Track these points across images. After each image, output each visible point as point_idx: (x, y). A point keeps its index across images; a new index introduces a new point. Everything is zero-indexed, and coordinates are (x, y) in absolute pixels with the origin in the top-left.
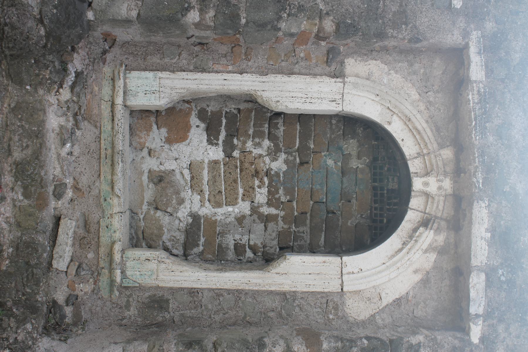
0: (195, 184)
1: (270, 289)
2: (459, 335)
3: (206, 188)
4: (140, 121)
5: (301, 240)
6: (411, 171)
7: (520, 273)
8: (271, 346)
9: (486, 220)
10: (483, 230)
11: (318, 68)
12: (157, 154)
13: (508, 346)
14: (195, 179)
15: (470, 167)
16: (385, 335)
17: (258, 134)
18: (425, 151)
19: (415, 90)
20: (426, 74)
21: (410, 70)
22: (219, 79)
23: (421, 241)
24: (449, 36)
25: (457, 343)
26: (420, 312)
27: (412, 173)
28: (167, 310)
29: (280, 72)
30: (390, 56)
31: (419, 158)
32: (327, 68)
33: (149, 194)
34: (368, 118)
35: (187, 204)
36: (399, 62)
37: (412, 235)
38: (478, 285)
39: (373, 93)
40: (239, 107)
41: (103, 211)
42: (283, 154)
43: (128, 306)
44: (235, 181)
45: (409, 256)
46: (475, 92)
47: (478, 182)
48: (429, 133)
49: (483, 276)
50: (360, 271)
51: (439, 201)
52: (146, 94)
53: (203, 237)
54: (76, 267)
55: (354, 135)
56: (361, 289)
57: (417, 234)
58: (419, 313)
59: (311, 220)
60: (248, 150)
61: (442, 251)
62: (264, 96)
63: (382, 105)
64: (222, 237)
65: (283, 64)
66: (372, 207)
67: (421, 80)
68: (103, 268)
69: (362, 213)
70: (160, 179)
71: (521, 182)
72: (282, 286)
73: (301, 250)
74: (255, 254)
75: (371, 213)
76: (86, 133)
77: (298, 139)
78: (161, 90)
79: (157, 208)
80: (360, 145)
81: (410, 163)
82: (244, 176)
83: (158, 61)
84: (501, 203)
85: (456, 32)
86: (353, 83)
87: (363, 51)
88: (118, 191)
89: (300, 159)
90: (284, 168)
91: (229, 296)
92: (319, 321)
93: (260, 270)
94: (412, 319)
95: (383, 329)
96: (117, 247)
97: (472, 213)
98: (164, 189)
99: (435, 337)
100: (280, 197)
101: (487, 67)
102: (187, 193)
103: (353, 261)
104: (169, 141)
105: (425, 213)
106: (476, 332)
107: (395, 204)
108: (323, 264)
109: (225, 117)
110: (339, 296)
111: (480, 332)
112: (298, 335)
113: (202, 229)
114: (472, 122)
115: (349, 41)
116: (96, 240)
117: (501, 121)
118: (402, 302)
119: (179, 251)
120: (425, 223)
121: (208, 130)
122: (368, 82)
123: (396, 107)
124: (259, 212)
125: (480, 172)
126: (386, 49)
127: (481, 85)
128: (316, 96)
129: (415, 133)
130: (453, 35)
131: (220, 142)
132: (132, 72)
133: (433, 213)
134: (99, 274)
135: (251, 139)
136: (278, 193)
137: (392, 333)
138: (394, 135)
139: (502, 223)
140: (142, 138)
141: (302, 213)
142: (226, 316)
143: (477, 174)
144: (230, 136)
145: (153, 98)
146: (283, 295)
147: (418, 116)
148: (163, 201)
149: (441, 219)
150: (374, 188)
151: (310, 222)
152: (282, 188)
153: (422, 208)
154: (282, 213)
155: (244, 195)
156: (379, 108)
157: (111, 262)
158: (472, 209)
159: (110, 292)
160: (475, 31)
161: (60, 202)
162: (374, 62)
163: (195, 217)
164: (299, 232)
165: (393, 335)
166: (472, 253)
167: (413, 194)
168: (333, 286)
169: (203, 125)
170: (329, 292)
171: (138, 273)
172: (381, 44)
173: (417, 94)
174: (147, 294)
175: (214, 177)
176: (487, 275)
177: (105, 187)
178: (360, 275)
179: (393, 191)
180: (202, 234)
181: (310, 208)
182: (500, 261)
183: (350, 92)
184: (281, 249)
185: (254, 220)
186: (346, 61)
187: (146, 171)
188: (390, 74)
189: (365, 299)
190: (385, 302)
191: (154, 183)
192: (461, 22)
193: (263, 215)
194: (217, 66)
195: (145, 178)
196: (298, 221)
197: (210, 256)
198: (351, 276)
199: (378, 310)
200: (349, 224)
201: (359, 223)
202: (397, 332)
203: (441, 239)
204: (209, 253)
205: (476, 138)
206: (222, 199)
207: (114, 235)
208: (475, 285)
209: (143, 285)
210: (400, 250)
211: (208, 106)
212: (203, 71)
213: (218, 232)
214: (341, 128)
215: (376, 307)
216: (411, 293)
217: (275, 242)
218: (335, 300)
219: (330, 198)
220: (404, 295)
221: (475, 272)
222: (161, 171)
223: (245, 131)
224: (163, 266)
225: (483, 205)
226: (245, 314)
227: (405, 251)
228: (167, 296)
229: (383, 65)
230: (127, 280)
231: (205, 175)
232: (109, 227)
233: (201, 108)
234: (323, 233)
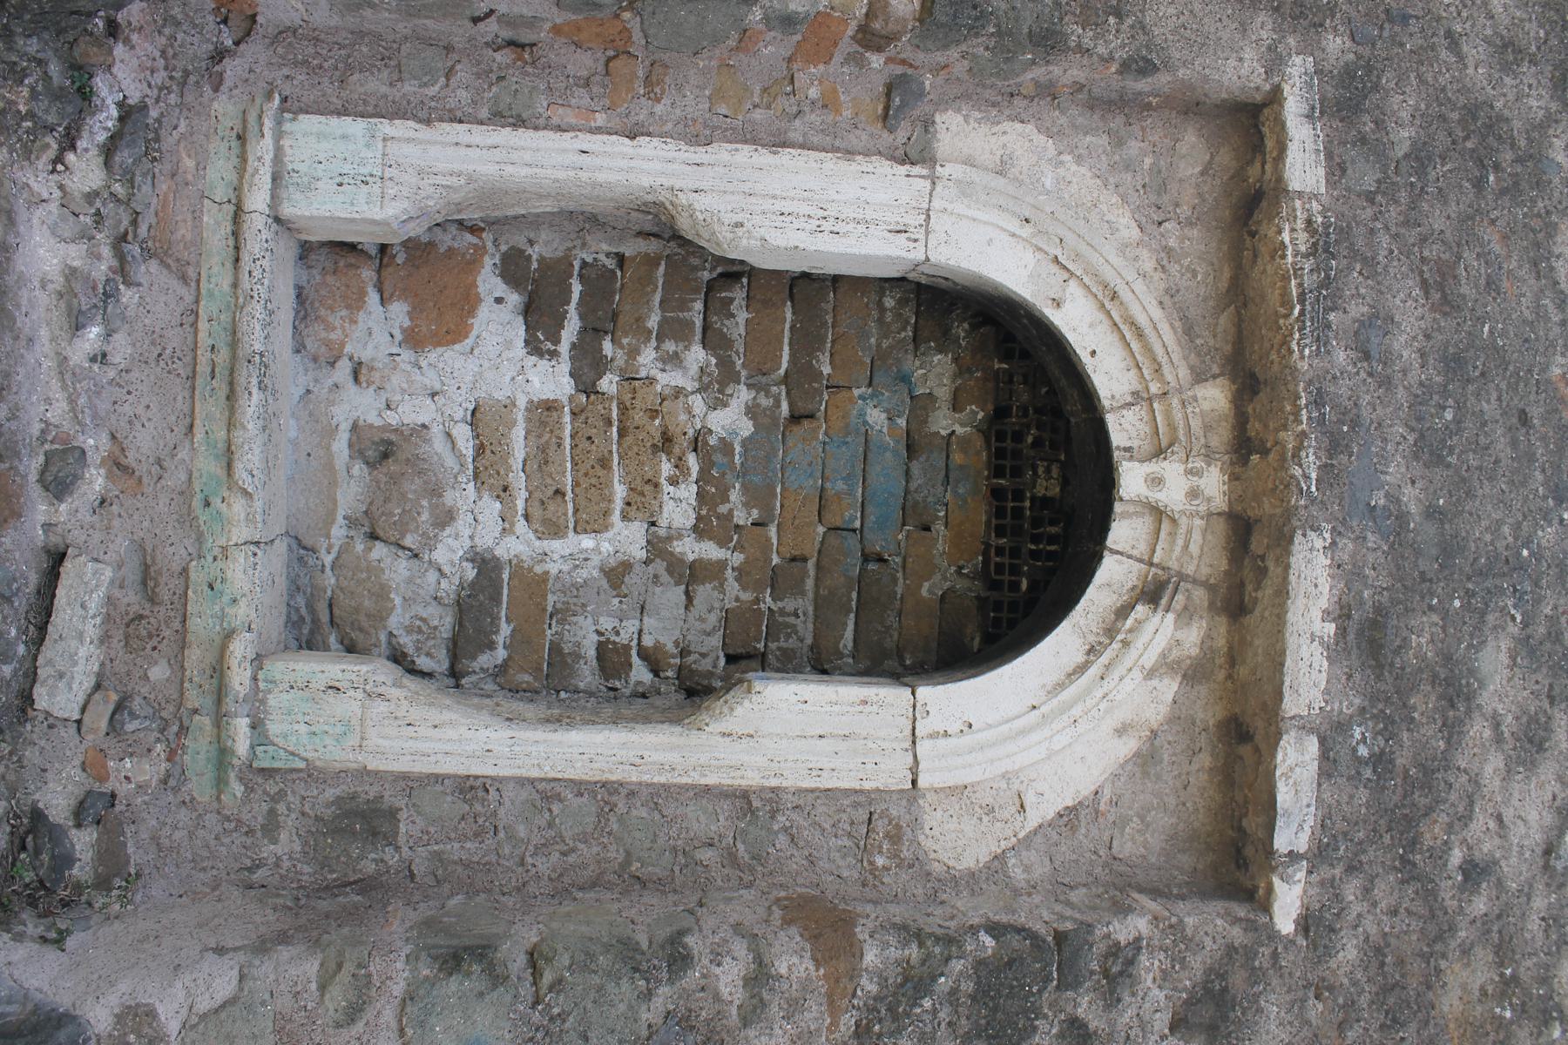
0: (487, 465)
1: (703, 781)
2: (1241, 911)
3: (518, 481)
4: (330, 279)
5: (788, 636)
6: (1114, 444)
7: (1405, 735)
8: (706, 962)
10: (1316, 614)
11: (858, 132)
12: (376, 375)
13: (1367, 939)
14: (488, 452)
15: (1282, 434)
16: (1040, 916)
17: (674, 330)
18: (1154, 388)
19: (1128, 214)
22: (565, 151)
23: (1140, 642)
24: (1232, 62)
25: (1237, 934)
26: (1129, 844)
27: (1118, 448)
28: (391, 840)
29: (749, 137)
30: (1063, 113)
31: (1137, 408)
32: (885, 134)
33: (351, 493)
34: (997, 286)
35: (463, 524)
36: (1086, 134)
38: (1298, 770)
39: (1014, 214)
40: (621, 250)
41: (200, 539)
42: (743, 388)
43: (271, 827)
44: (604, 463)
45: (1107, 685)
46: (1300, 224)
47: (1307, 477)
48: (1166, 338)
49: (1313, 746)
50: (966, 729)
51: (1189, 532)
52: (340, 185)
53: (508, 621)
54: (111, 707)
55: (945, 341)
56: (967, 781)
57: (1129, 622)
58: (1126, 847)
59: (817, 579)
60: (643, 374)
61: (1193, 673)
62: (697, 206)
63: (1040, 249)
64: (561, 622)
65: (758, 115)
66: (987, 546)
67: (1144, 186)
68: (196, 711)
69: (961, 563)
70: (383, 450)
71: (1413, 482)
72: (739, 773)
73: (788, 665)
74: (656, 674)
75: (986, 562)
76: (152, 296)
77: (786, 348)
78: (387, 175)
79: (373, 536)
80: (962, 370)
81: (1110, 419)
82: (630, 448)
83: (384, 89)
84: (1365, 538)
85: (1248, 54)
86: (959, 182)
87: (988, 94)
88: (244, 475)
89: (791, 405)
90: (746, 428)
91: (579, 800)
92: (845, 874)
93: (671, 722)
94: (1105, 865)
95: (1029, 894)
96: (240, 648)
97: (1287, 567)
98: (394, 479)
99: (1181, 921)
100: (731, 510)
101: (1329, 156)
102: (463, 495)
104: (414, 340)
105: (1151, 564)
106: (1288, 901)
107: (1052, 539)
108: (861, 708)
109: (581, 276)
110: (904, 802)
111: (1298, 903)
112: (787, 922)
113: (505, 598)
114: (1292, 308)
115: (954, 53)
116: (177, 625)
117: (1366, 309)
118: (1082, 817)
119: (438, 662)
120: (1152, 593)
121: (528, 311)
122: (1000, 182)
123: (1078, 256)
124: (672, 554)
125: (1311, 451)
126: (1048, 92)
127: (1314, 204)
128: (852, 215)
130: (1241, 60)
131: (564, 348)
132: (301, 117)
133: (1173, 565)
134: (183, 730)
135: (654, 343)
136: (725, 499)
137: (1058, 908)
138: (1071, 337)
139: (1366, 594)
140: (334, 329)
141: (793, 559)
142: (571, 859)
143: (1303, 454)
144: (592, 332)
145: (362, 198)
146: (743, 799)
147: (1139, 286)
148: (392, 514)
149: (1195, 581)
150: (997, 493)
151: (817, 586)
152: (737, 486)
153: (1142, 549)
154: (738, 559)
155: (629, 504)
156: (1029, 257)
157: (220, 692)
158: (1288, 553)
159: (218, 785)
160: (1298, 54)
161: (63, 507)
162: (1018, 126)
163: (486, 565)
164: (782, 612)
165: (1062, 918)
168: (890, 774)
169: (514, 299)
170: (878, 790)
171: (303, 728)
172: (1038, 72)
174: (330, 793)
175: (543, 449)
176: (1322, 741)
177: (207, 466)
178: (967, 739)
179: (1045, 502)
180: (503, 613)
181: (817, 546)
182: (1357, 701)
183: (950, 207)
184: (731, 659)
185: (656, 576)
186: (938, 118)
187: (345, 426)
188: (1061, 163)
189: (977, 808)
190: (1034, 819)
191: (368, 463)
193: (682, 561)
194: (561, 111)
195: (341, 445)
196: (778, 582)
197: (527, 678)
198: (942, 742)
199: (1014, 840)
200: (924, 592)
201: (951, 590)
202: (1068, 903)
203: (1192, 638)
204: (522, 670)
205: (1301, 352)
206: (566, 514)
207: (230, 611)
208: (1291, 769)
209: (318, 763)
210: (1081, 669)
211: (531, 242)
212: (519, 122)
213: (550, 609)
214: (908, 323)
215: (1010, 833)
216: (1107, 793)
217: (716, 641)
218: (894, 813)
219: (872, 518)
220: (1086, 798)
221: (1293, 733)
222: (387, 428)
223: (637, 320)
224: (381, 707)
225: (1319, 544)
226: (628, 854)
227: (1094, 671)
228: (392, 798)
229: (1043, 138)
230: (270, 748)
231: (518, 444)
232: (217, 586)
233: (512, 248)
234: (852, 616)
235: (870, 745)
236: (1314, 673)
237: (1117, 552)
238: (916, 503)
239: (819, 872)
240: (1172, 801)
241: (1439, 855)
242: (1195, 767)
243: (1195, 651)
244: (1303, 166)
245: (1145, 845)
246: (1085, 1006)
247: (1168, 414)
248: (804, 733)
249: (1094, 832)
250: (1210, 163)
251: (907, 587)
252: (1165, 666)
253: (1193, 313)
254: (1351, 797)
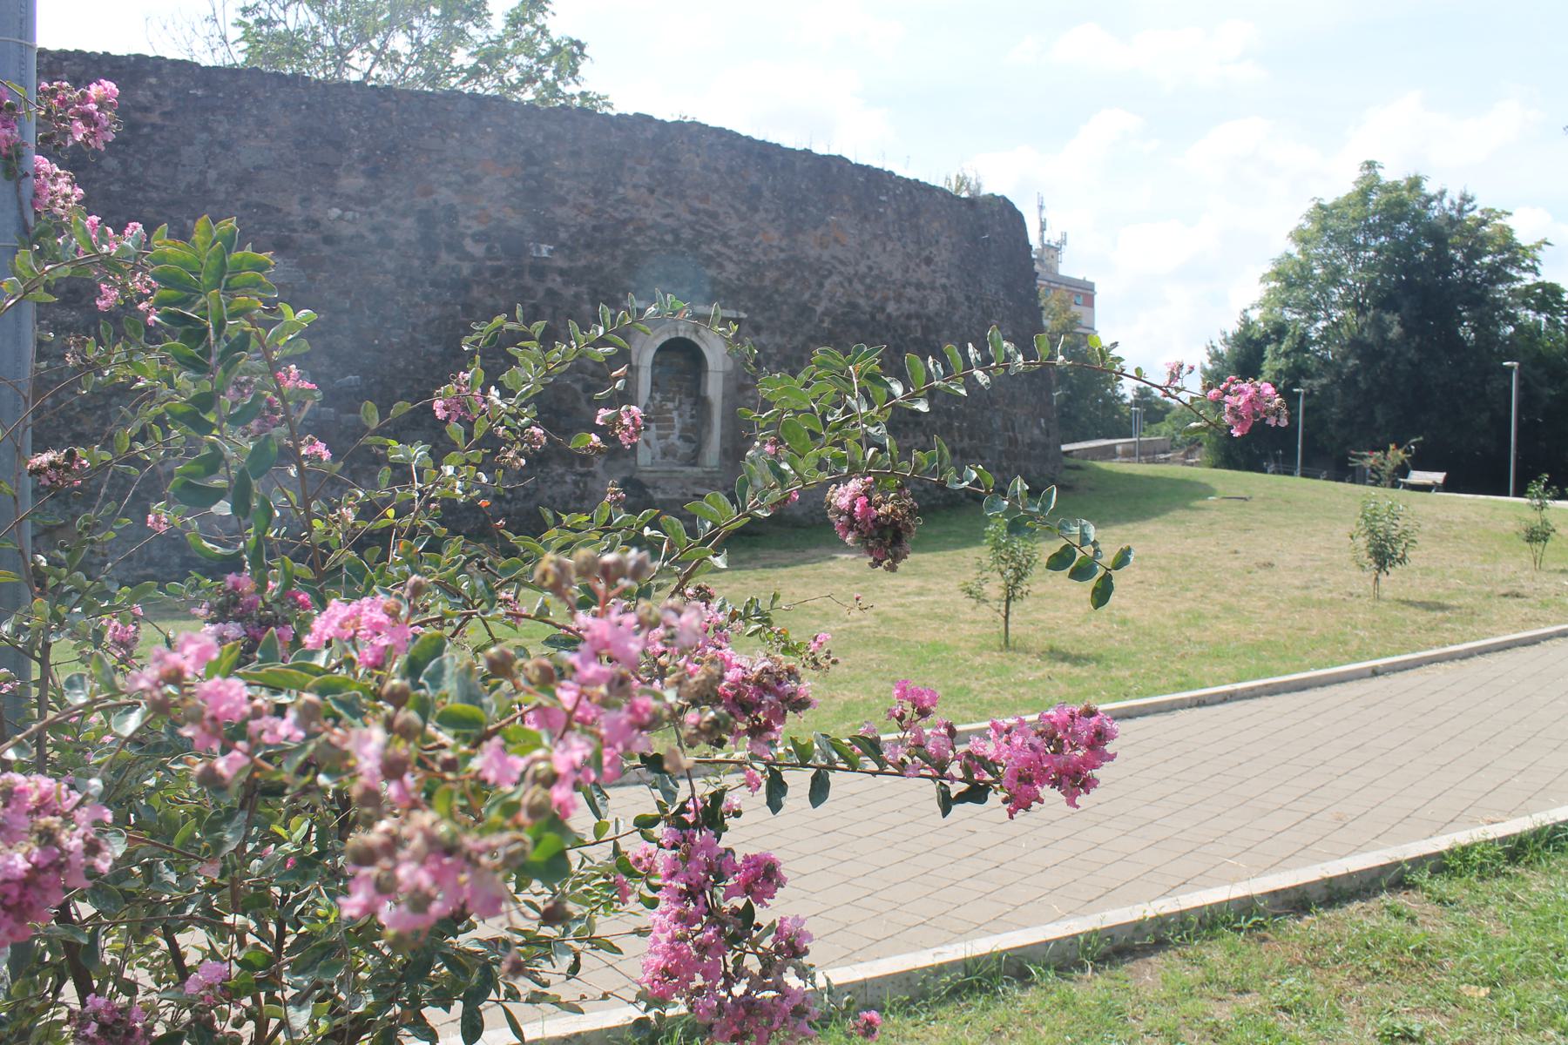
0: (666, 437)
37: (701, 338)
70: (665, 454)
73: (698, 386)
76: (661, 483)
103: (711, 366)
106: (743, 315)
196: (680, 387)
248: (714, 388)
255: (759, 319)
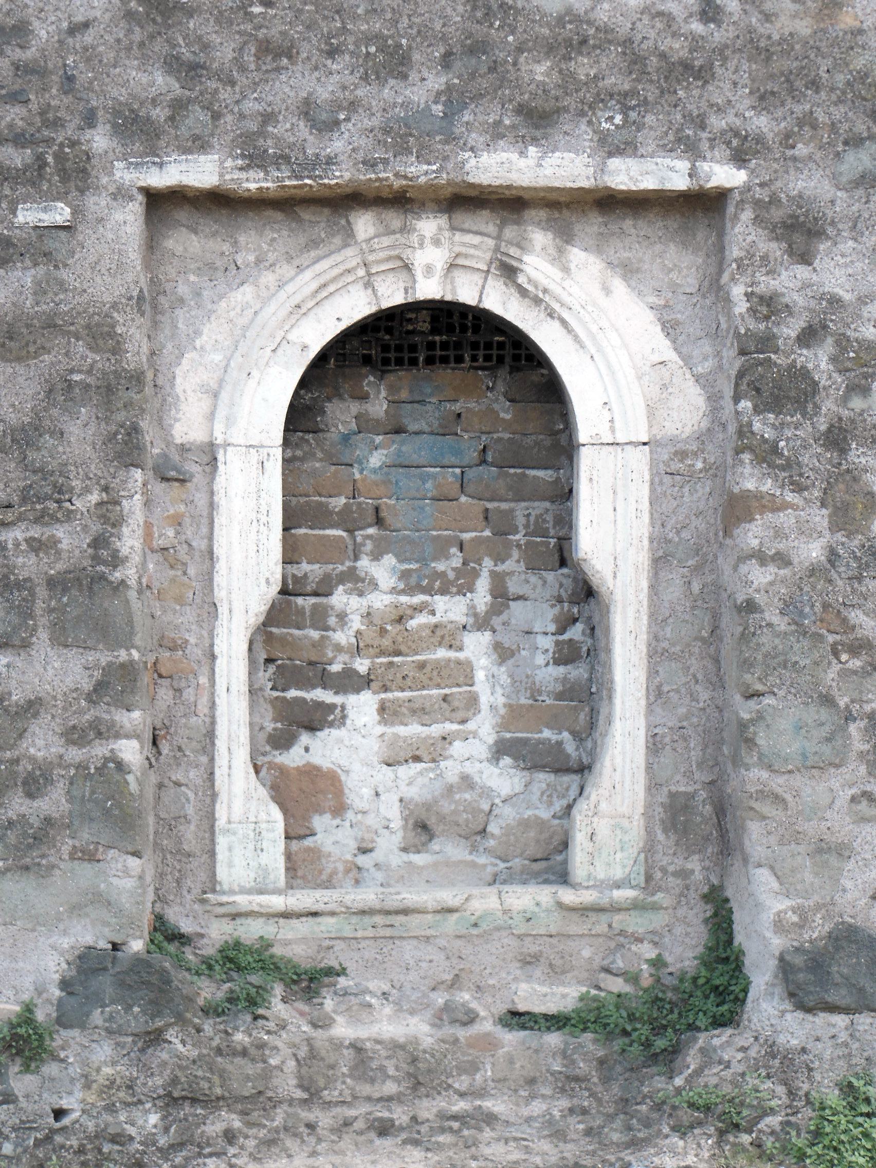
1: (646, 590)
3: (436, 730)
4: (300, 873)
5: (544, 521)
6: (403, 302)
9: (505, 155)
10: (522, 163)
11: (196, 500)
12: (367, 836)
13: (754, 108)
14: (417, 753)
17: (319, 618)
19: (233, 294)
20: (199, 269)
21: (192, 303)
22: (228, 703)
23: (544, 282)
25: (747, 215)
26: (688, 279)
28: (692, 796)
29: (208, 578)
30: (164, 347)
32: (195, 480)
33: (450, 849)
35: (470, 768)
36: (176, 327)
37: (533, 298)
38: (632, 174)
40: (262, 661)
41: (498, 929)
42: (359, 564)
43: (683, 874)
44: (422, 666)
45: (576, 307)
46: (243, 175)
47: (426, 173)
49: (615, 163)
52: (262, 850)
53: (541, 732)
54: (609, 977)
56: (643, 406)
57: (530, 288)
58: (691, 282)
59: (501, 500)
60: (354, 640)
61: (566, 236)
62: (256, 611)
64: (540, 693)
65: (191, 571)
66: (471, 367)
68: (610, 926)
69: (484, 387)
70: (421, 828)
72: (640, 566)
74: (575, 620)
77: (329, 532)
78: (254, 820)
79: (483, 831)
81: (386, 304)
82: (409, 648)
84: (467, 123)
86: (228, 426)
88: (457, 899)
89: (370, 526)
90: (389, 560)
91: (661, 672)
92: (708, 489)
93: (608, 612)
94: (704, 297)
96: (568, 896)
98: (442, 819)
99: (735, 260)
100: (454, 569)
102: (451, 770)
103: (588, 420)
104: (339, 809)
105: (488, 271)
108: (595, 482)
109: (283, 690)
110: (659, 449)
111: (726, 167)
112: (731, 536)
113: (525, 735)
114: (306, 185)
116: (554, 941)
117: (301, 123)
118: (669, 318)
119: (572, 780)
120: (509, 272)
121: (312, 728)
122: (224, 396)
124: (487, 612)
128: (255, 502)
129: (324, 294)
131: (338, 700)
133: (488, 256)
134: (622, 933)
135: (330, 633)
136: (443, 574)
139: (507, 122)
140: (335, 868)
141: (486, 518)
142: (700, 677)
143: (410, 175)
144: (325, 680)
147: (290, 288)
148: (467, 820)
150: (430, 361)
151: (506, 501)
152: (433, 565)
153: (478, 278)
154: (488, 563)
155: (451, 646)
157: (598, 909)
159: (657, 909)
162: (178, 380)
163: (501, 749)
164: (526, 526)
166: (569, 185)
167: (449, 298)
168: (639, 462)
169: (305, 738)
170: (651, 469)
171: (619, 855)
173: (241, 289)
174: (661, 836)
175: (414, 712)
176: (610, 155)
180: (536, 736)
181: (475, 501)
182: (583, 127)
184: (563, 563)
185: (504, 624)
186: (178, 441)
187: (405, 857)
191: (430, 840)
192: (96, 203)
193: (492, 604)
194: (199, 707)
195: (419, 859)
197: (582, 716)
198: (617, 425)
200: (508, 417)
203: (540, 238)
204: (576, 719)
205: (337, 177)
206: (460, 693)
207: (544, 905)
208: (631, 178)
209: (641, 845)
210: (564, 322)
211: (262, 728)
212: (211, 734)
213: (531, 702)
214: (302, 438)
216: (652, 299)
217: (550, 576)
218: (666, 457)
219: (453, 459)
221: (606, 178)
222: (405, 828)
223: (314, 646)
224: (603, 806)
225: (473, 162)
226: (696, 639)
227: (566, 315)
228: (662, 797)
229: (184, 361)
230: (632, 876)
231: (413, 730)
232: (528, 915)
233: (268, 742)
234: (528, 472)
235: (620, 475)
236: (565, 163)
237: (481, 297)
238: (440, 426)
239: (706, 514)
240: (658, 247)
241: (696, 43)
242: (633, 231)
243: (550, 235)
244: (201, 172)
245: (689, 268)
246: (790, 330)
247: (379, 262)
249: (680, 307)
250: (188, 227)
251: (504, 430)
252: (559, 259)
253: (302, 240)
254: (651, 128)
255: (810, 184)
